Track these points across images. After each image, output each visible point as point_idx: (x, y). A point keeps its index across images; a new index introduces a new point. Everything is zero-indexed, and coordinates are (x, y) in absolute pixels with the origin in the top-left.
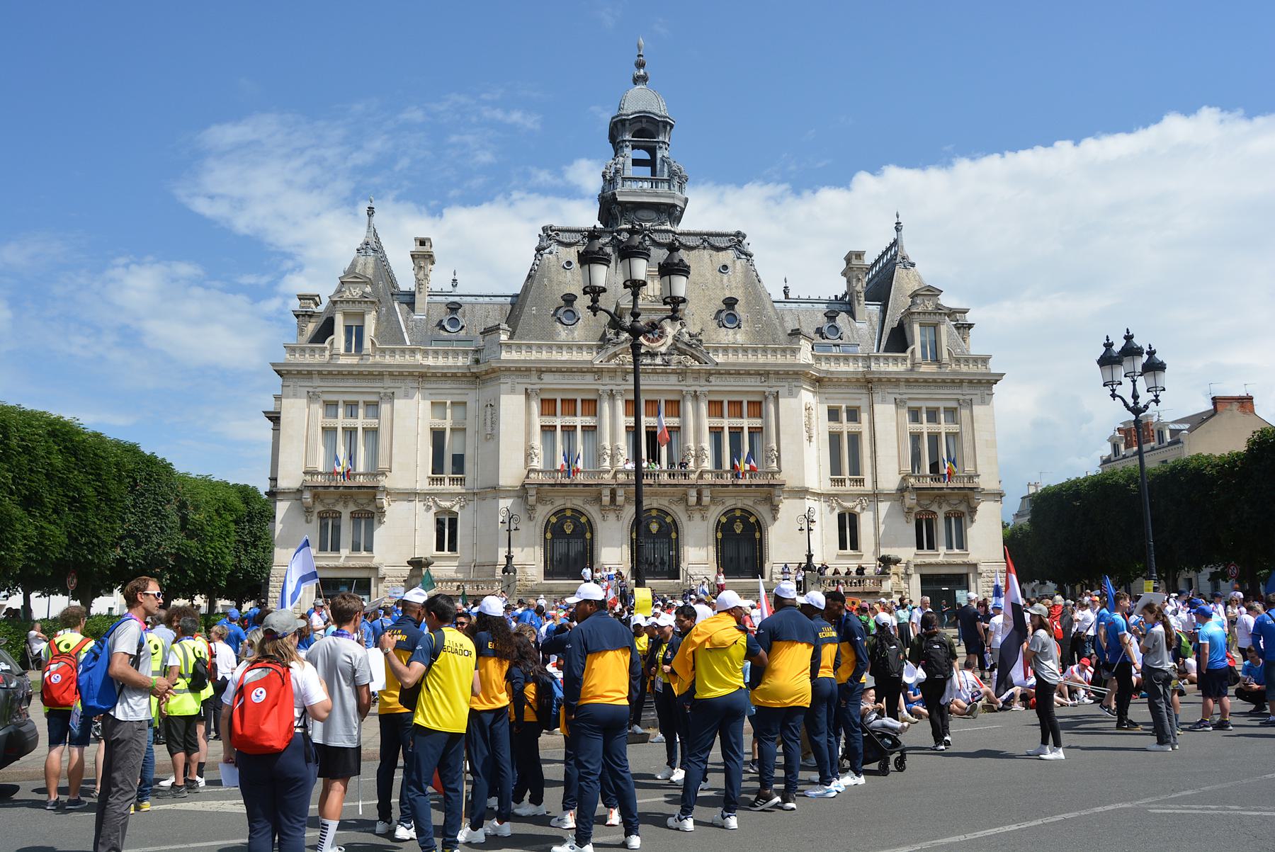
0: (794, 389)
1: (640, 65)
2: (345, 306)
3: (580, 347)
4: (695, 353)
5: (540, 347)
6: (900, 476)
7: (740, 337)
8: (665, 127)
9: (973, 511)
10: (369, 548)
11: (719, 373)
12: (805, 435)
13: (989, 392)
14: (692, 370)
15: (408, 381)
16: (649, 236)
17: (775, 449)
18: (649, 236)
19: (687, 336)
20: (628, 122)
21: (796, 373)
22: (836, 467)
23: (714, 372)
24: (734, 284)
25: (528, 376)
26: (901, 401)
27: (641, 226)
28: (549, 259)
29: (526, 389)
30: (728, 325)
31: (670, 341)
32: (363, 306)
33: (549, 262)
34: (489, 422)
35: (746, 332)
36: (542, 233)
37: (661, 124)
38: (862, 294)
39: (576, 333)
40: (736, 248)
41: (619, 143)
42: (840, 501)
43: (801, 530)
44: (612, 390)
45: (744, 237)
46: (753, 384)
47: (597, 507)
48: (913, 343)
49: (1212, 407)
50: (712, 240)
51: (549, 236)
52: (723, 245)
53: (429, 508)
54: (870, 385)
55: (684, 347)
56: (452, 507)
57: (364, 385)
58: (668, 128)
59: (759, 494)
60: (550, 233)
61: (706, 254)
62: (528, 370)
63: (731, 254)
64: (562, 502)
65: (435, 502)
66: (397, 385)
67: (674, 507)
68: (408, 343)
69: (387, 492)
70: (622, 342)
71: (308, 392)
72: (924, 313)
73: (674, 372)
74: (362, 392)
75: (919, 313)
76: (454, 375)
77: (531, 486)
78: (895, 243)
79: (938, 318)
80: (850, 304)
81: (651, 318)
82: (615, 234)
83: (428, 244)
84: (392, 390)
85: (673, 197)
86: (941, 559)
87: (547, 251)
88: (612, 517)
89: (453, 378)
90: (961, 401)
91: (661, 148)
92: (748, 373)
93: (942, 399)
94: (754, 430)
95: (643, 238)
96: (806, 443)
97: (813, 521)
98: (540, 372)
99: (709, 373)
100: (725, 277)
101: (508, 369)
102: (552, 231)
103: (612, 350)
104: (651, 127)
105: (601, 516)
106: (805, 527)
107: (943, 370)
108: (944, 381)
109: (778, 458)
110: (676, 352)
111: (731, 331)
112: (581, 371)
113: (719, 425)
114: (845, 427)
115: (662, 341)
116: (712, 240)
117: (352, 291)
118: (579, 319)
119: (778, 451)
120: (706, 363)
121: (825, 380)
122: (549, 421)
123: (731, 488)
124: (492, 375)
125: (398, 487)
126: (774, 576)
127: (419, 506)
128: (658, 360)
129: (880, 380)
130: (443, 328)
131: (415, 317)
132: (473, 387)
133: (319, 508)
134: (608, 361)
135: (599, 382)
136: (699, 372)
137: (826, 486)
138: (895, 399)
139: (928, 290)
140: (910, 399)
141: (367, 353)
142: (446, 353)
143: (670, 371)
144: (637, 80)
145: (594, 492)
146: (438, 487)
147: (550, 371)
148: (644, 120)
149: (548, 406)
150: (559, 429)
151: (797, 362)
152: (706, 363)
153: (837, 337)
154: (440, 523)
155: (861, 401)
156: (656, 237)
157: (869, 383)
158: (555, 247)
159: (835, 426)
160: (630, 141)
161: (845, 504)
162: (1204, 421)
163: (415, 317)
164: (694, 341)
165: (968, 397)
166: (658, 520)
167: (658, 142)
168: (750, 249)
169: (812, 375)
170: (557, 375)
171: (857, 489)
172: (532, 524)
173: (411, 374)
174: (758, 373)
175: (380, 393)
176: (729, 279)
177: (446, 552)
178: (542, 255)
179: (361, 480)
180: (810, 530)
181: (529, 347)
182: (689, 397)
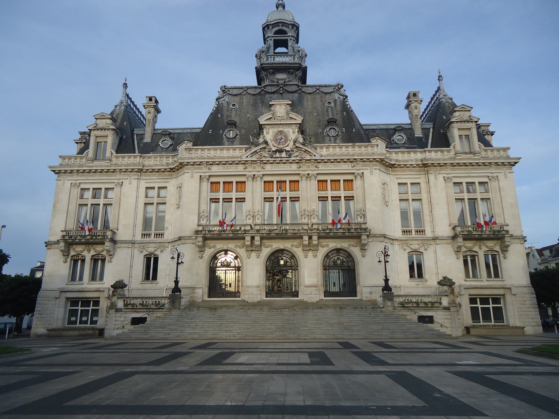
9: (505, 249)
13: (510, 171)
16: (282, 88)
18: (282, 88)
20: (271, 27)
26: (448, 178)
27: (278, 82)
28: (222, 103)
29: (201, 176)
31: (291, 144)
33: (222, 106)
36: (220, 90)
37: (290, 26)
43: (380, 261)
44: (254, 175)
45: (342, 86)
46: (346, 167)
47: (243, 250)
50: (321, 89)
53: (141, 252)
54: (426, 169)
55: (301, 146)
56: (156, 251)
57: (105, 177)
62: (201, 164)
66: (125, 177)
67: (294, 249)
72: (461, 122)
75: (457, 122)
78: (439, 88)
81: (280, 130)
86: (485, 283)
97: (388, 255)
103: (254, 149)
104: (285, 28)
106: (382, 259)
116: (321, 89)
122: (214, 195)
126: (363, 295)
128: (284, 154)
133: (72, 253)
138: (444, 177)
148: (281, 25)
152: (315, 156)
155: (422, 180)
156: (288, 88)
158: (227, 98)
160: (273, 37)
161: (412, 247)
163: (144, 141)
165: (495, 175)
167: (289, 36)
168: (346, 93)
169: (386, 162)
170: (221, 167)
172: (201, 260)
180: (386, 262)
182: (304, 178)
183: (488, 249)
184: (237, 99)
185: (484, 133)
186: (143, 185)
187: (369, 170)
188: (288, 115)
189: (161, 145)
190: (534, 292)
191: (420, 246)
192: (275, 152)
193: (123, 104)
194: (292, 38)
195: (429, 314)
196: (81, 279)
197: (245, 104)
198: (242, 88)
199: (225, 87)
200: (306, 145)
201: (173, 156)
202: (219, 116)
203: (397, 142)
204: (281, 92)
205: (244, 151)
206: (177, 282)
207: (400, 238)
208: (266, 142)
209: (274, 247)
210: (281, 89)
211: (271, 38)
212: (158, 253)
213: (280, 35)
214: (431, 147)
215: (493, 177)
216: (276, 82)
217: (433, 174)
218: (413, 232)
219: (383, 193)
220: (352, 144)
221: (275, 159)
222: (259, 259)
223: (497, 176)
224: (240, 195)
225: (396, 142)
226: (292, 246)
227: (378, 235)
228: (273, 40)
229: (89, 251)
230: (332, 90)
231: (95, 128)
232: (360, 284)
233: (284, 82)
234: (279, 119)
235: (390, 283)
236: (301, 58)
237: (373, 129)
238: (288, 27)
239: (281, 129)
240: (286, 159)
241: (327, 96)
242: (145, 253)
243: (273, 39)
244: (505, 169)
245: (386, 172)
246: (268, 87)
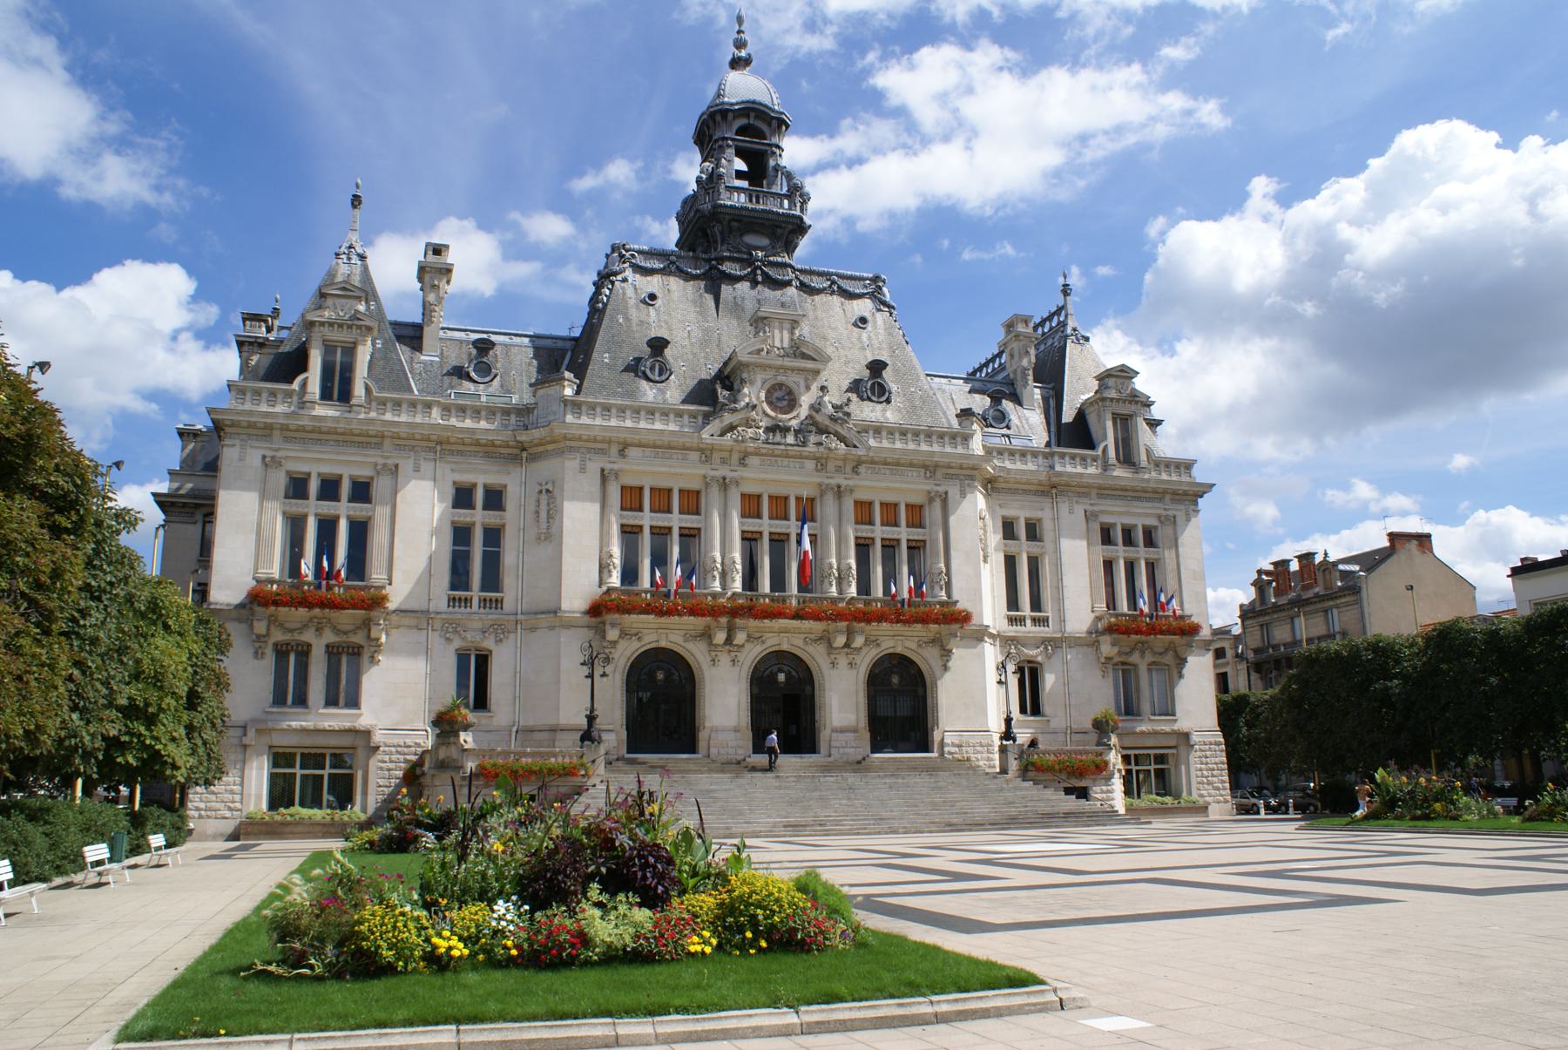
0: (967, 489)
1: (740, 44)
6: (1092, 616)
8: (779, 127)
10: (354, 702)
12: (982, 558)
19: (830, 406)
20: (730, 115)
22: (1013, 603)
24: (875, 342)
27: (751, 255)
29: (603, 470)
30: (873, 398)
33: (624, 294)
34: (543, 515)
37: (774, 123)
38: (1031, 372)
41: (716, 141)
48: (1105, 437)
49: (1388, 544)
51: (622, 256)
52: (857, 291)
55: (827, 422)
58: (784, 128)
60: (624, 252)
61: (836, 300)
64: (653, 637)
68: (416, 393)
71: (264, 457)
79: (1133, 408)
80: (1013, 384)
82: (713, 262)
87: (619, 277)
90: (1162, 518)
93: (1140, 515)
96: (982, 563)
99: (857, 464)
100: (864, 335)
102: (627, 251)
104: (764, 127)
105: (709, 659)
107: (1140, 476)
109: (948, 585)
111: (879, 407)
115: (794, 414)
119: (948, 574)
120: (855, 446)
121: (1001, 480)
124: (550, 447)
126: (946, 749)
128: (790, 439)
131: (423, 358)
134: (722, 435)
138: (1086, 512)
140: (1102, 512)
143: (806, 454)
144: (736, 63)
149: (632, 498)
152: (855, 446)
156: (772, 272)
157: (1052, 489)
158: (629, 273)
160: (733, 140)
162: (1382, 561)
164: (840, 415)
165: (1170, 513)
167: (770, 145)
178: (613, 283)
181: (607, 409)
184: (656, 279)
186: (452, 475)
188: (798, 348)
189: (473, 374)
190: (1222, 740)
192: (771, 429)
195: (1083, 784)
196: (301, 700)
197: (675, 296)
202: (621, 320)
203: (993, 424)
205: (700, 419)
206: (591, 719)
209: (769, 643)
212: (489, 643)
214: (1059, 445)
216: (744, 253)
218: (1028, 622)
223: (1174, 517)
232: (940, 725)
238: (770, 125)
239: (781, 378)
242: (457, 643)
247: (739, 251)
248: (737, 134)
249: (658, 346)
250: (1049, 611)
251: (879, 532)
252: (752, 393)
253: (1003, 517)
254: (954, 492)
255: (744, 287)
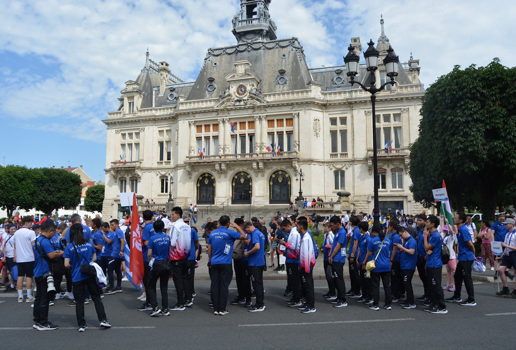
2: (127, 94)
3: (210, 101)
4: (258, 98)
5: (194, 102)
7: (286, 88)
11: (269, 106)
14: (257, 106)
15: (149, 123)
16: (250, 46)
17: (298, 141)
18: (250, 46)
21: (307, 103)
22: (334, 148)
23: (267, 106)
25: (189, 116)
28: (208, 63)
29: (189, 122)
31: (248, 94)
32: (133, 93)
35: (289, 86)
39: (213, 94)
40: (291, 45)
42: (334, 165)
43: (297, 180)
47: (216, 172)
51: (209, 53)
52: (285, 45)
53: (157, 175)
54: (352, 105)
55: (253, 96)
59: (289, 163)
60: (210, 51)
62: (188, 113)
63: (290, 48)
65: (159, 173)
69: (139, 168)
70: (226, 97)
73: (249, 108)
74: (132, 128)
76: (166, 119)
77: (187, 164)
81: (240, 84)
83: (164, 64)
84: (144, 127)
85: (261, 26)
86: (388, 193)
87: (208, 60)
88: (223, 176)
89: (166, 120)
91: (259, 4)
92: (283, 105)
94: (289, 132)
95: (248, 47)
96: (314, 138)
98: (193, 113)
100: (284, 60)
101: (181, 114)
102: (211, 50)
105: (218, 176)
108: (391, 100)
109: (299, 145)
110: (250, 98)
111: (282, 86)
112: (209, 112)
113: (272, 131)
114: (339, 126)
117: (130, 87)
118: (215, 88)
119: (299, 142)
122: (199, 134)
123: (271, 160)
125: (146, 167)
127: (153, 174)
129: (356, 102)
130: (168, 99)
132: (173, 123)
133: (119, 176)
135: (218, 116)
136: (259, 107)
137: (328, 158)
138: (365, 111)
139: (384, 52)
141: (135, 112)
142: (167, 109)
143: (247, 108)
145: (211, 164)
146: (161, 166)
147: (196, 113)
149: (199, 127)
150: (203, 138)
151: (309, 97)
153: (341, 83)
154: (162, 181)
156: (254, 46)
157: (350, 104)
158: (212, 58)
159: (334, 127)
160: (245, 4)
163: (159, 96)
164: (258, 93)
166: (282, 176)
169: (318, 103)
170: (201, 114)
171: (344, 158)
173: (149, 120)
174: (287, 105)
175: (139, 129)
176: (286, 61)
177: (165, 193)
179: (133, 164)
183: (394, 167)
185: (411, 69)
187: (304, 110)
191: (342, 166)
192: (237, 101)
193: (146, 69)
194: (260, 3)
197: (223, 62)
198: (222, 49)
199: (210, 49)
200: (257, 95)
201: (174, 107)
204: (249, 50)
207: (328, 160)
208: (229, 95)
209: (236, 170)
210: (249, 47)
211: (244, 5)
213: (250, 2)
215: (404, 109)
216: (246, 42)
217: (357, 109)
218: (339, 155)
219: (314, 127)
220: (292, 91)
221: (236, 107)
222: (226, 178)
223: (408, 109)
224: (216, 133)
225: (335, 84)
226: (248, 169)
227: (306, 159)
228: (245, 6)
229: (128, 175)
230: (287, 45)
231: (126, 92)
233: (252, 41)
234: (240, 75)
235: (303, 194)
236: (265, 20)
237: (322, 72)
239: (241, 83)
240: (244, 106)
241: (284, 49)
243: (246, 4)
244: (415, 102)
245: (320, 110)
246: (240, 47)
247: (244, 42)
248: (247, 1)
249: (211, 80)
250: (349, 152)
251: (276, 129)
252: (233, 89)
253: (330, 118)
254: (301, 112)
255: (245, 53)
